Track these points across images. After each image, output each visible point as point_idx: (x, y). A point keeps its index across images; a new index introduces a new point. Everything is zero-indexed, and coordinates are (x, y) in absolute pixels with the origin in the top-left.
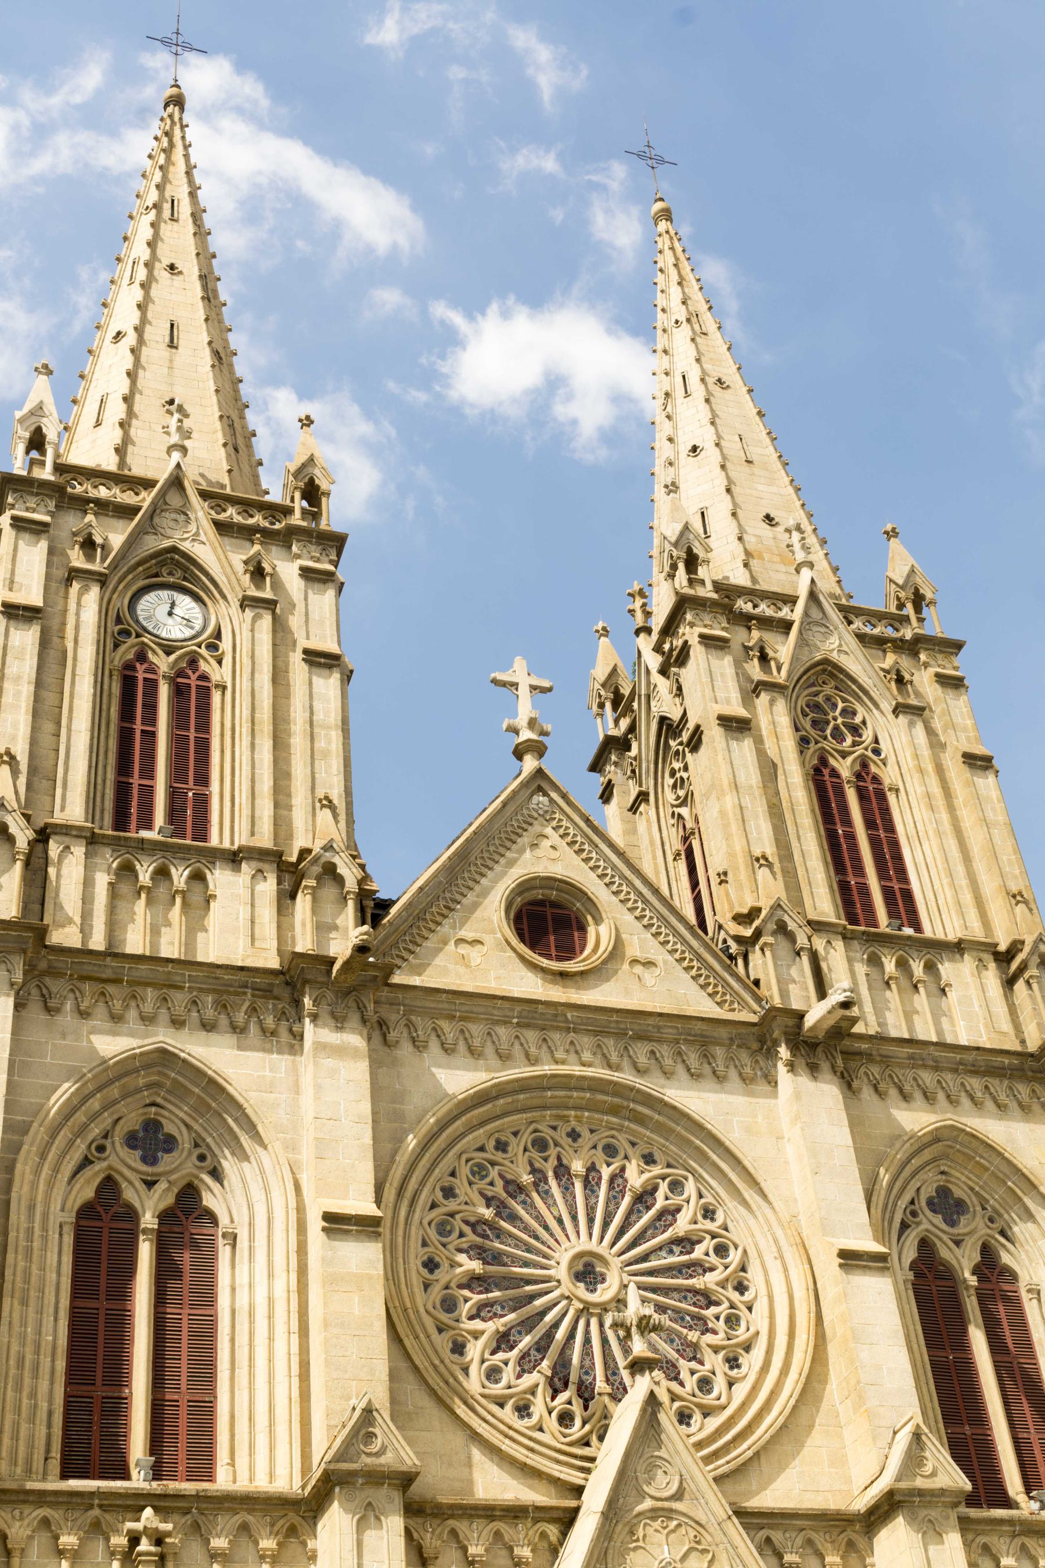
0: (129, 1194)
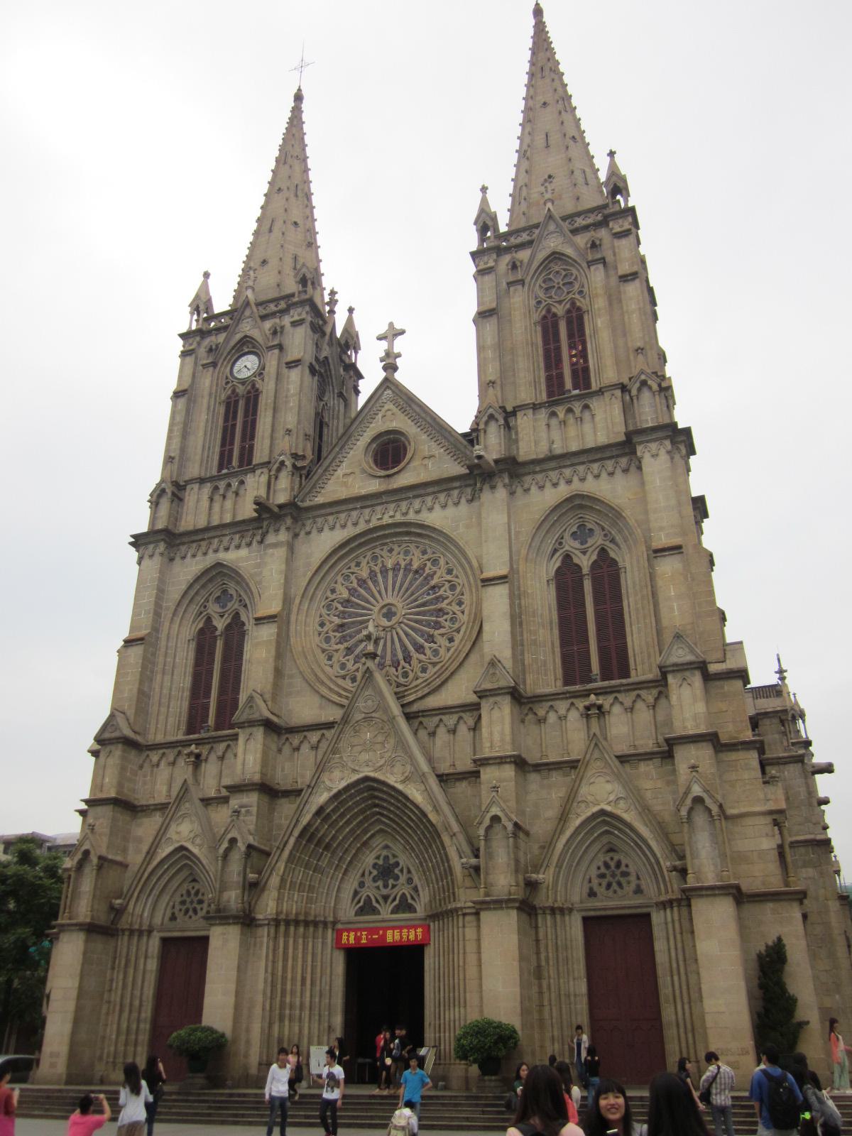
0: (215, 623)
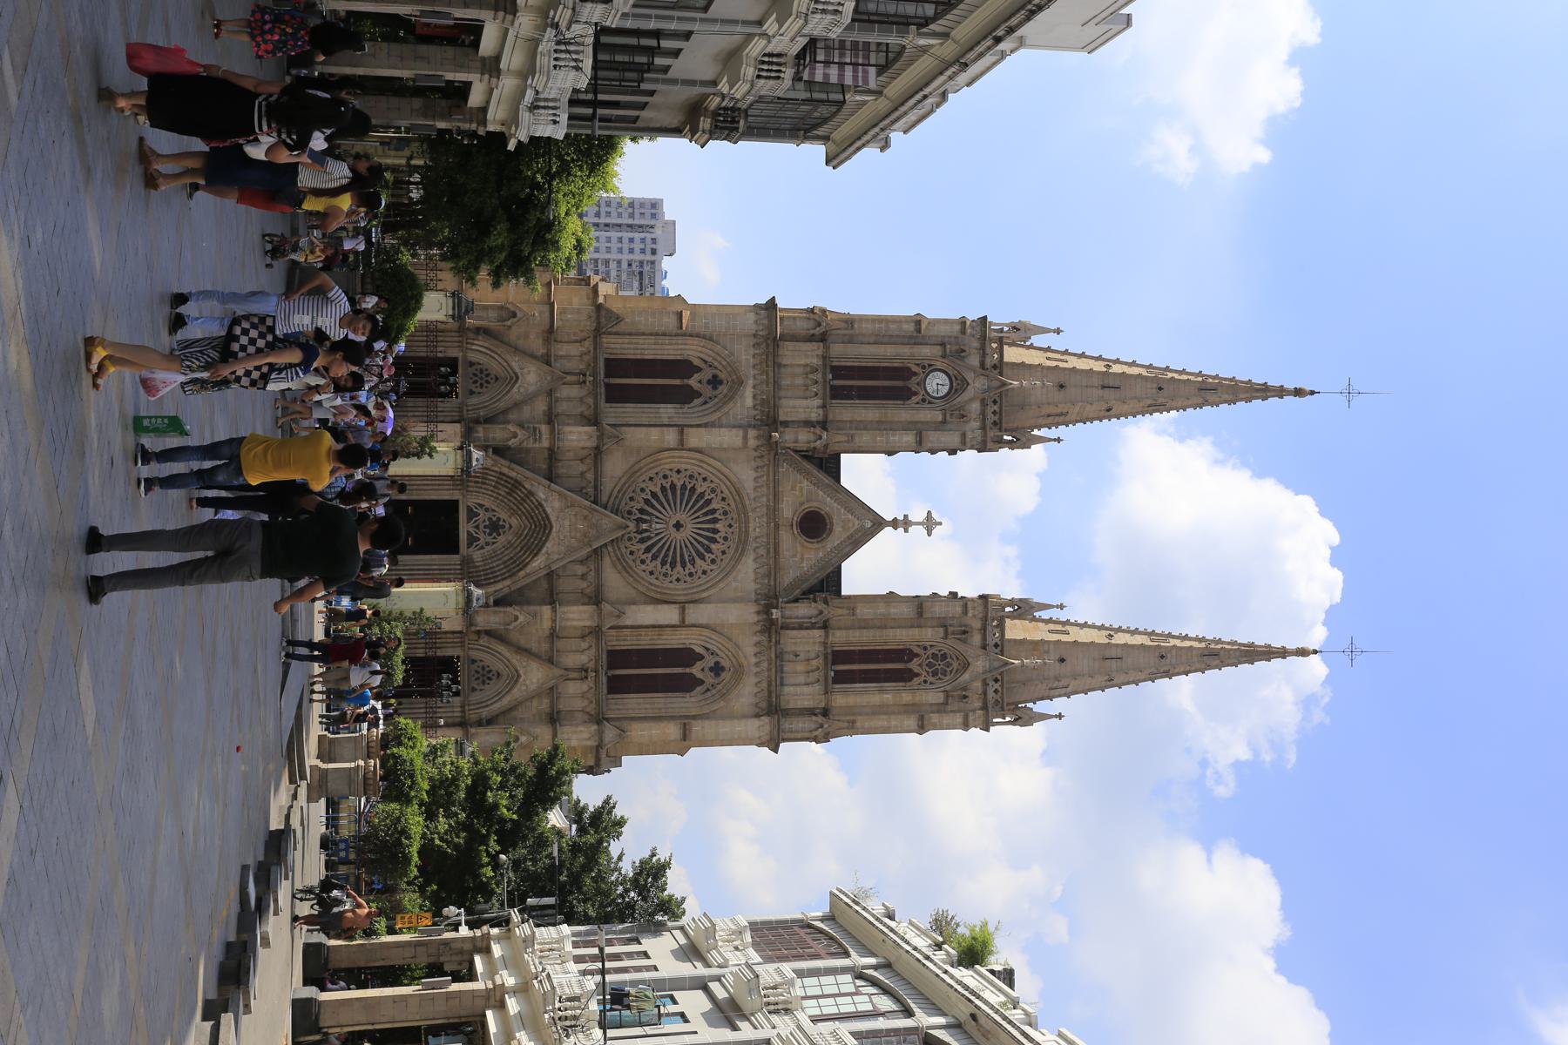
0: (696, 376)
